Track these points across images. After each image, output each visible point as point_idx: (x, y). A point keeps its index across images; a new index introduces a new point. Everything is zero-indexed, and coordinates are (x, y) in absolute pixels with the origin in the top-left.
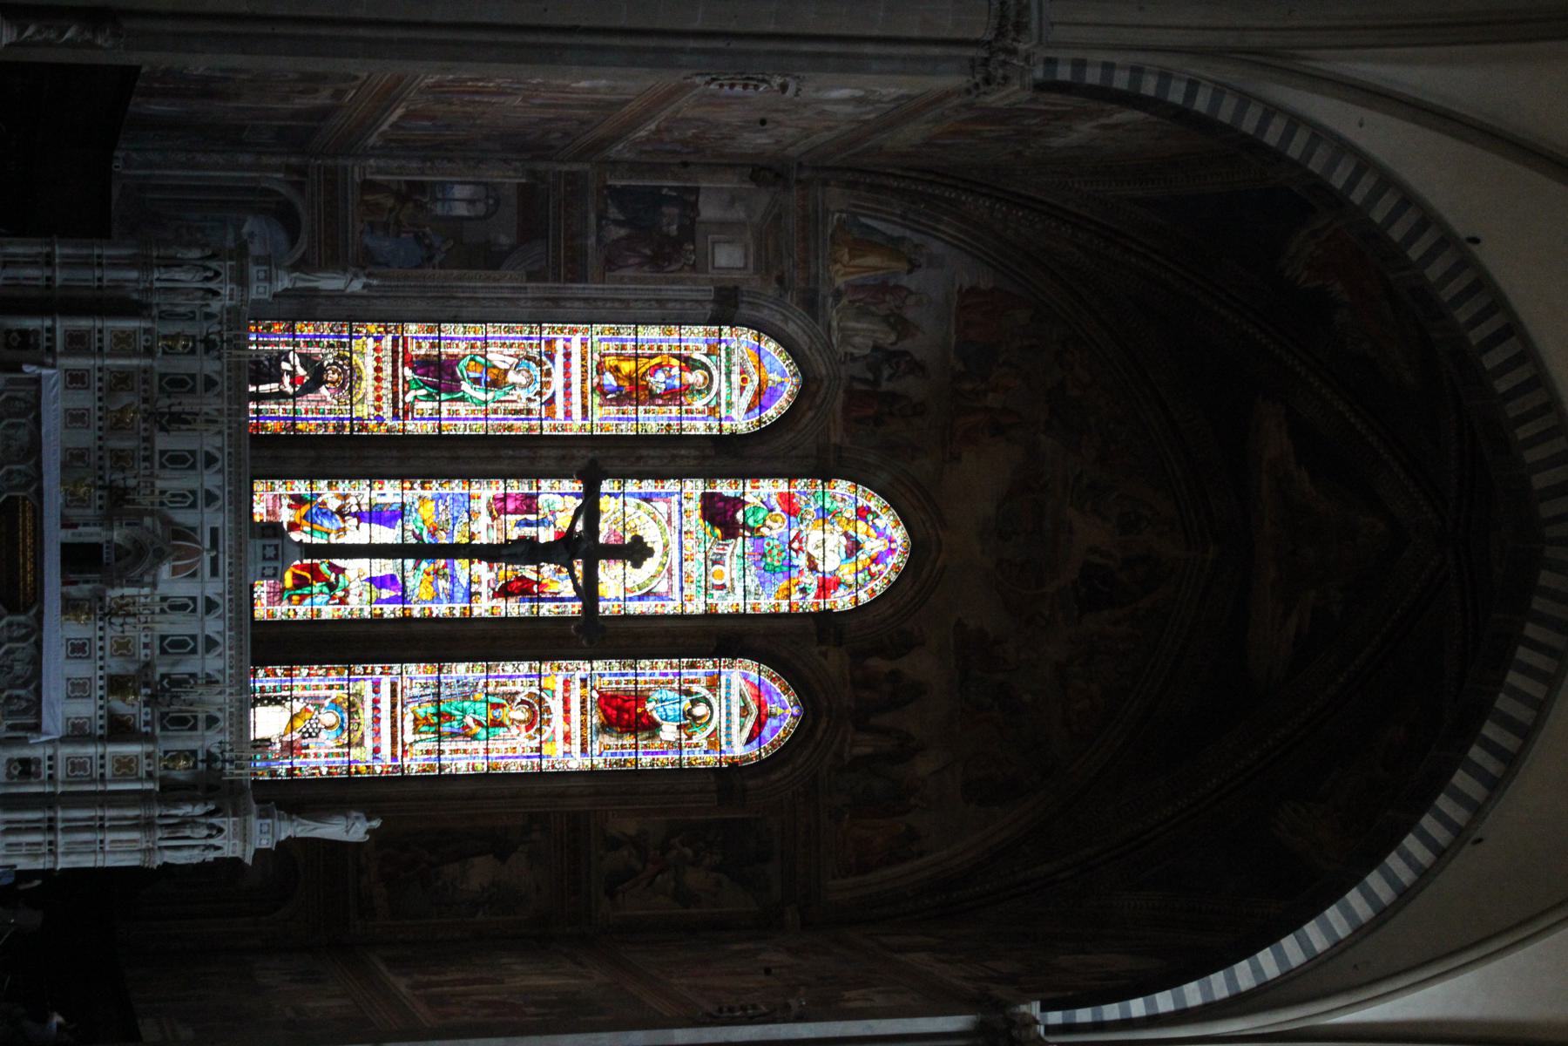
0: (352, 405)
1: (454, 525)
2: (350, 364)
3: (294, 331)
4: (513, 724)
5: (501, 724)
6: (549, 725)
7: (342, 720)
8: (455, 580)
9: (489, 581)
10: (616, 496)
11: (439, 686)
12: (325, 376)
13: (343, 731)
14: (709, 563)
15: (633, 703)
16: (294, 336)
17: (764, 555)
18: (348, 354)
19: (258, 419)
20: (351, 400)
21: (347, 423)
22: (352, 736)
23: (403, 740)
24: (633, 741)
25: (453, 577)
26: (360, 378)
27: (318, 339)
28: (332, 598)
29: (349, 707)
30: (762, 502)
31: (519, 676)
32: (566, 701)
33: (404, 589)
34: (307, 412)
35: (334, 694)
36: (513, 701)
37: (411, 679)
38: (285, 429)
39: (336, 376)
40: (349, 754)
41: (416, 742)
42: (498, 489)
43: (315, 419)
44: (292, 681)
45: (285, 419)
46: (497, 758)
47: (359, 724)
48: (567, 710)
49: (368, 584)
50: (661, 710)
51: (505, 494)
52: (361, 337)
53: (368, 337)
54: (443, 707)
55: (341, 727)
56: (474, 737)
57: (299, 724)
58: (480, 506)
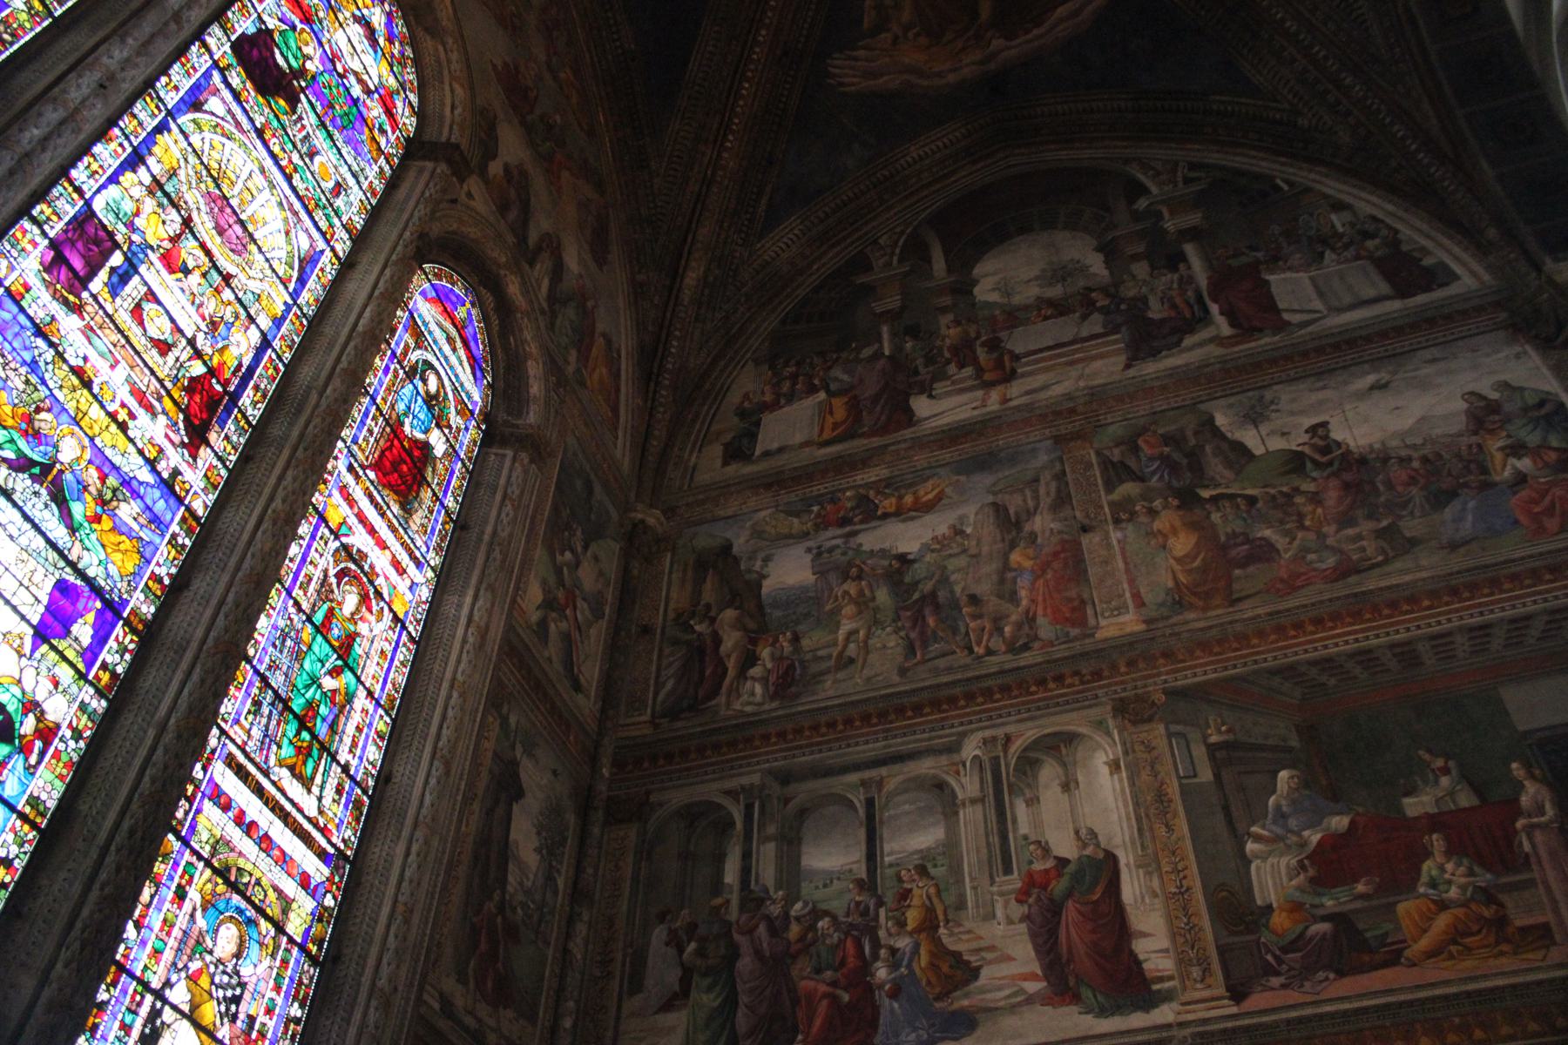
1: (44, 382)
4: (356, 623)
5: (351, 638)
6: (378, 575)
7: (240, 911)
8: (135, 484)
9: (167, 436)
10: (162, 128)
11: (268, 685)
13: (257, 925)
14: (307, 160)
15: (396, 442)
17: (332, 107)
22: (269, 911)
23: (309, 819)
24: (430, 493)
25: (126, 483)
28: (26, 750)
29: (227, 882)
30: (280, 20)
31: (309, 546)
32: (362, 518)
33: (97, 591)
35: (194, 895)
36: (332, 592)
37: (237, 721)
40: (291, 940)
41: (320, 799)
42: (35, 245)
44: (131, 975)
46: (383, 689)
47: (258, 883)
48: (372, 531)
49: (44, 648)
50: (415, 422)
51: (54, 244)
54: (297, 705)
55: (251, 922)
56: (350, 698)
57: (209, 1012)
58: (42, 303)
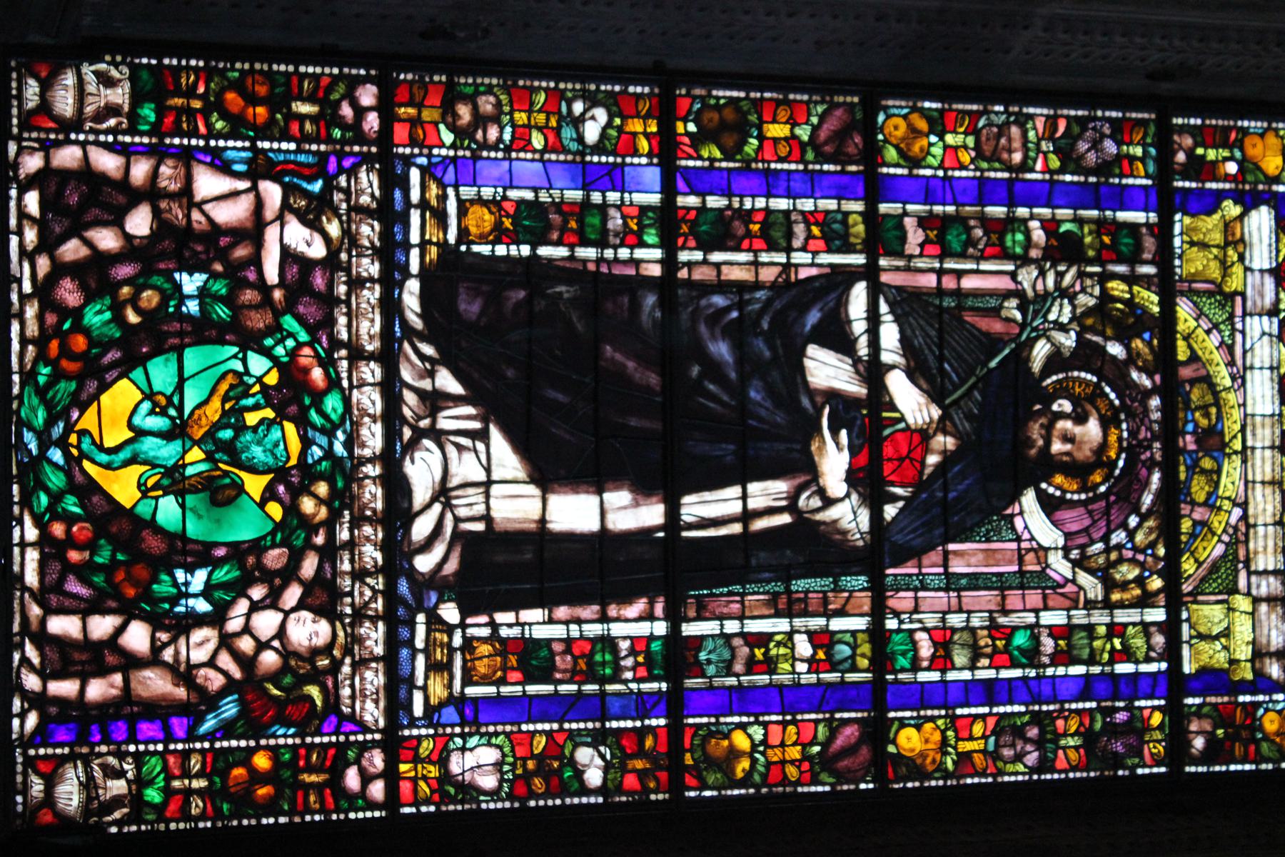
0: (1175, 601)
2: (1164, 361)
3: (872, 155)
12: (1035, 431)
16: (875, 188)
18: (1150, 300)
19: (675, 704)
20: (1172, 573)
21: (1152, 709)
26: (1213, 442)
27: (998, 211)
34: (942, 660)
38: (827, 762)
39: (1093, 428)
43: (990, 692)
45: (824, 697)
52: (1210, 203)
53: (1249, 202)
